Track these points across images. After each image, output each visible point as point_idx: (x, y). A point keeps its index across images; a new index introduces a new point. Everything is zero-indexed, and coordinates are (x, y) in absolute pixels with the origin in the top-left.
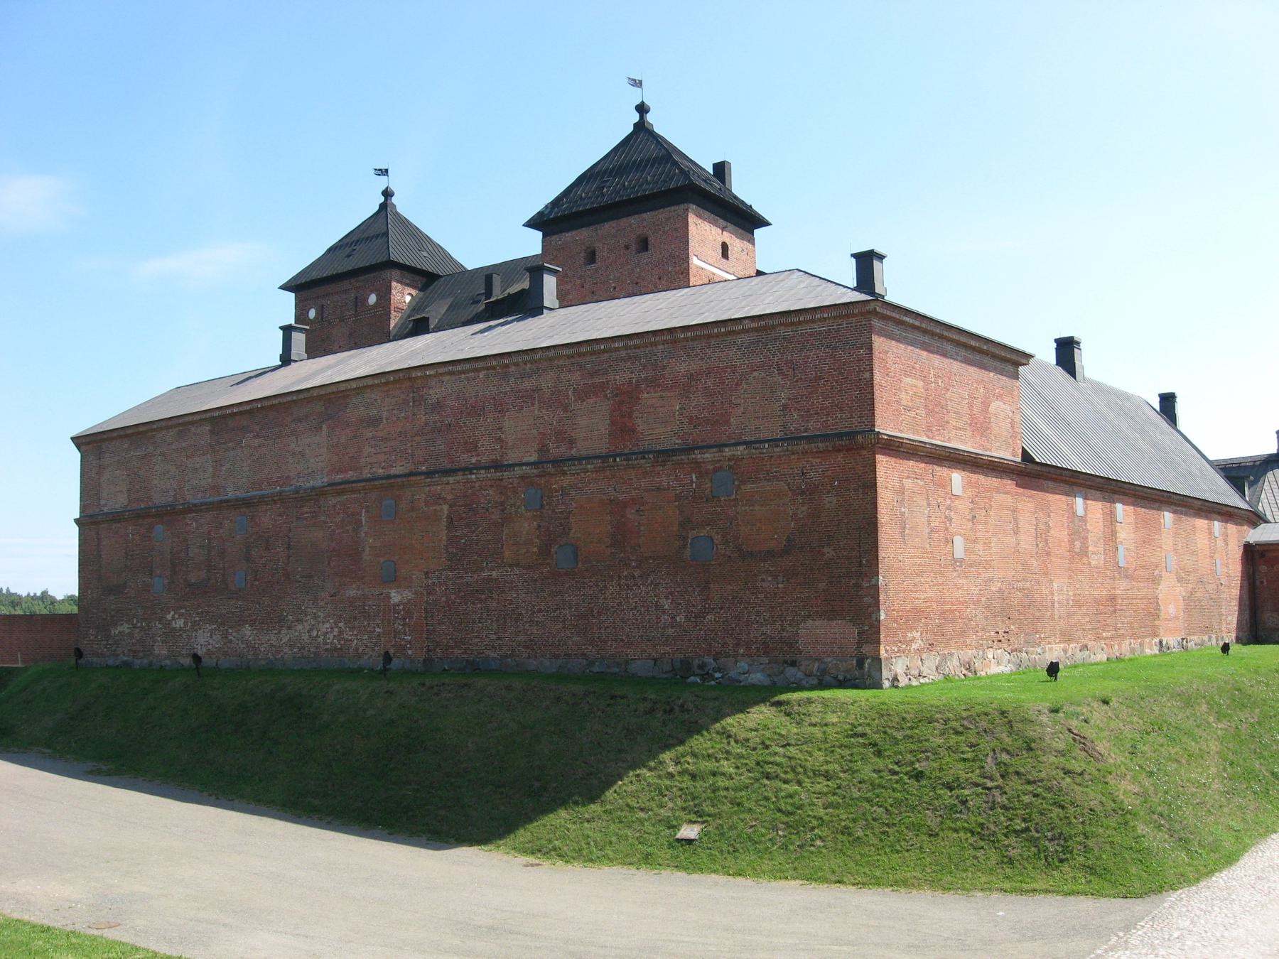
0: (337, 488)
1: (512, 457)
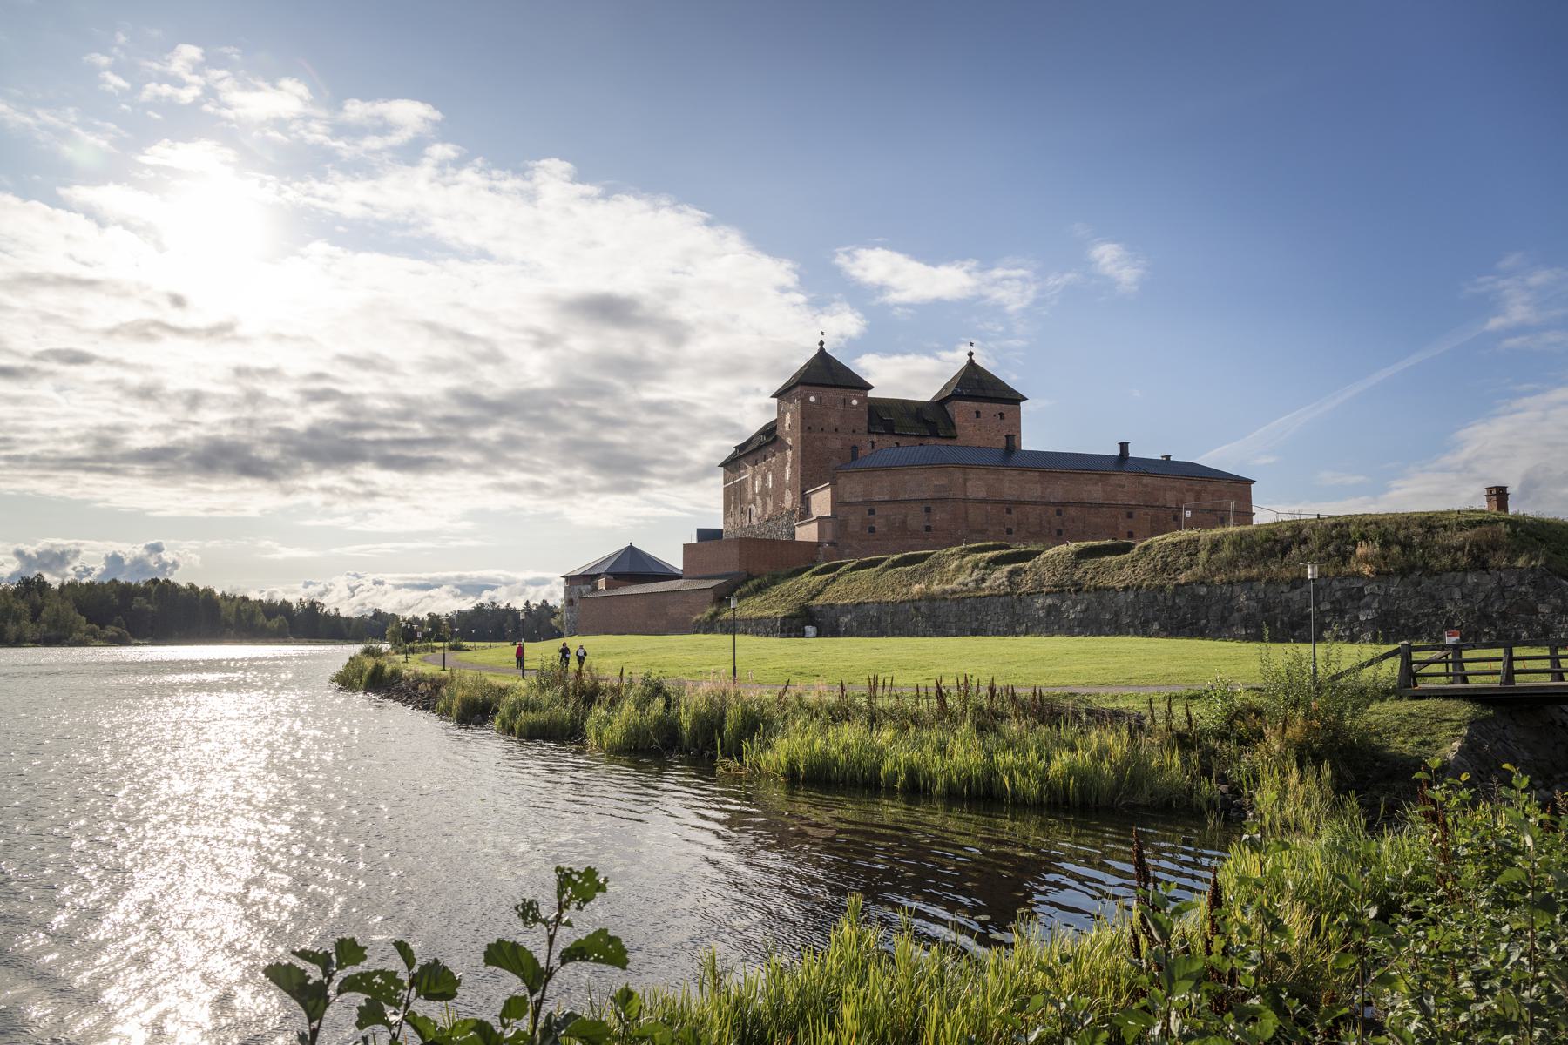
0: (1109, 506)
1: (1168, 505)
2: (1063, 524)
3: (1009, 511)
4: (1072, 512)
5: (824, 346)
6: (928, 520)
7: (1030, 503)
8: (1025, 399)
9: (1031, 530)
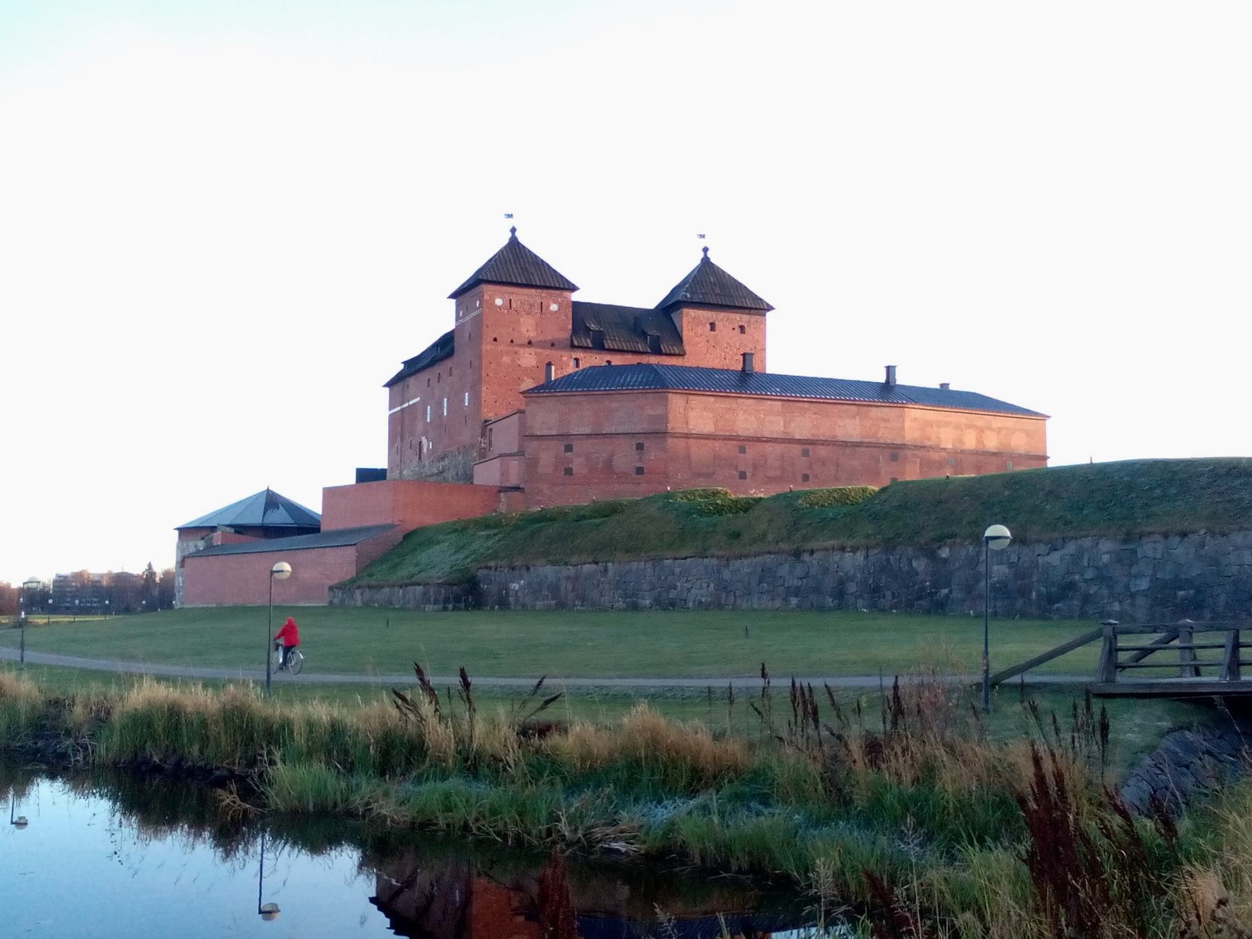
2: (810, 466)
3: (742, 450)
4: (823, 451)
5: (517, 234)
6: (640, 458)
7: (769, 440)
8: (770, 308)
9: (771, 474)
